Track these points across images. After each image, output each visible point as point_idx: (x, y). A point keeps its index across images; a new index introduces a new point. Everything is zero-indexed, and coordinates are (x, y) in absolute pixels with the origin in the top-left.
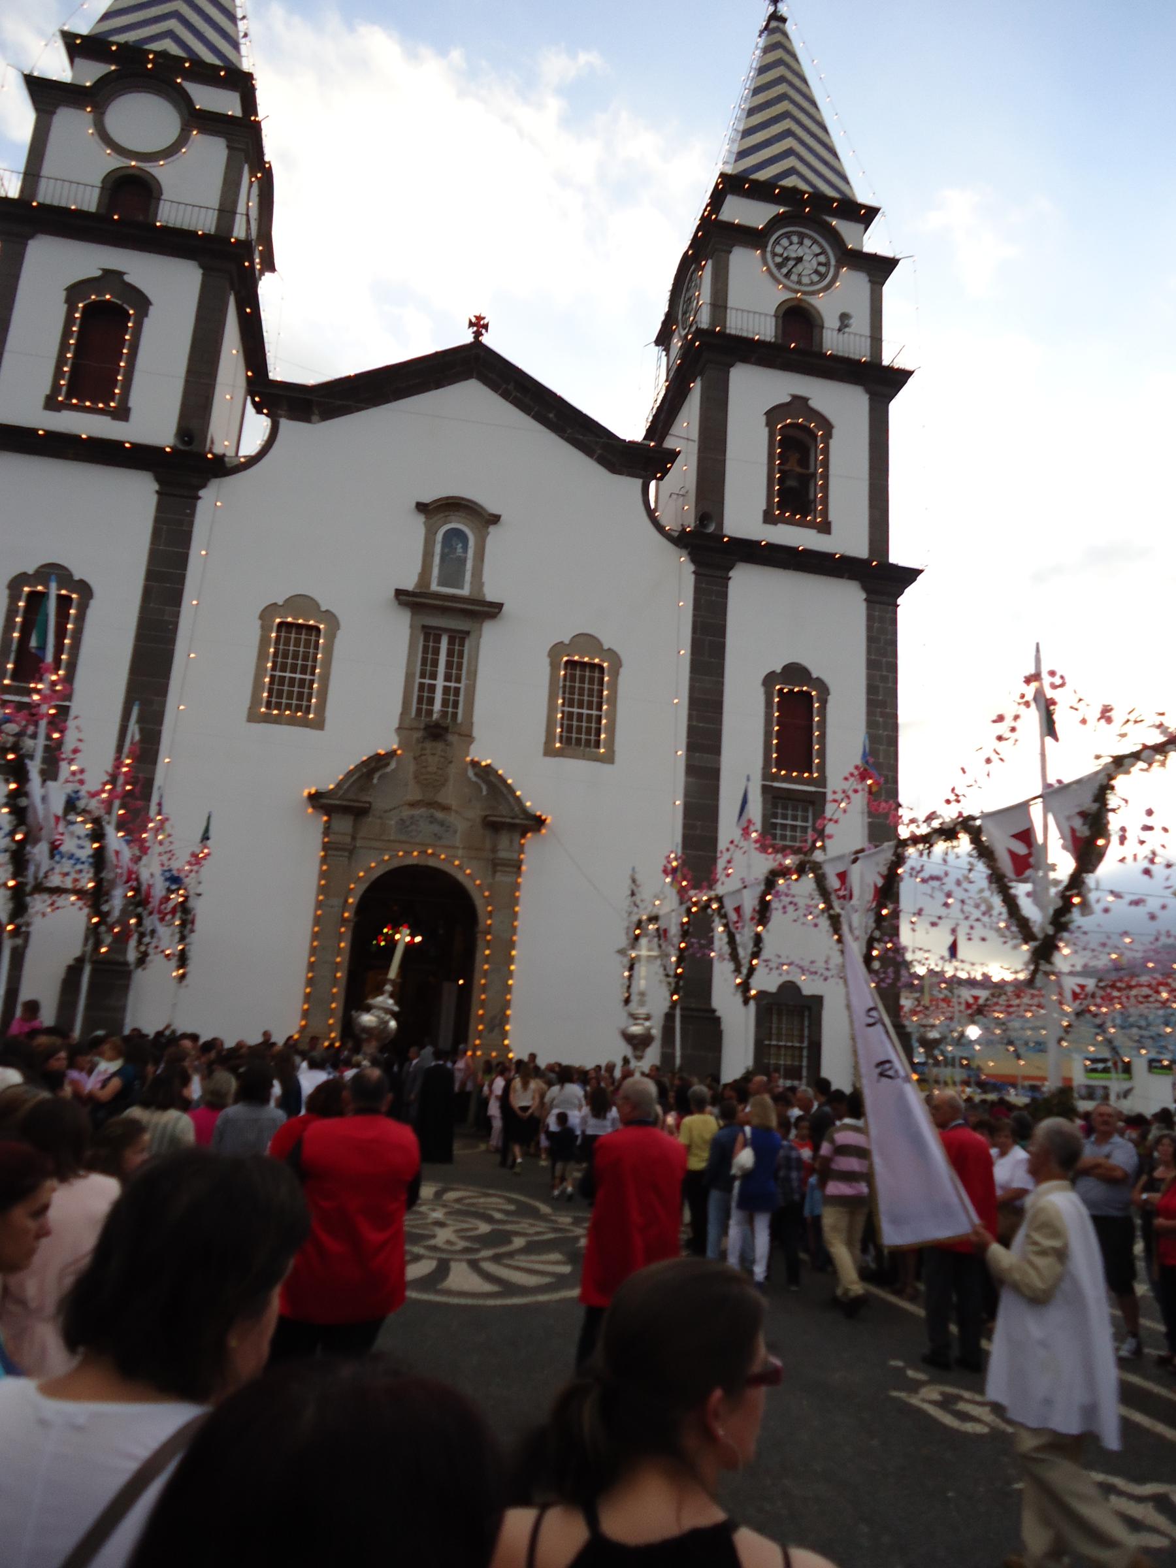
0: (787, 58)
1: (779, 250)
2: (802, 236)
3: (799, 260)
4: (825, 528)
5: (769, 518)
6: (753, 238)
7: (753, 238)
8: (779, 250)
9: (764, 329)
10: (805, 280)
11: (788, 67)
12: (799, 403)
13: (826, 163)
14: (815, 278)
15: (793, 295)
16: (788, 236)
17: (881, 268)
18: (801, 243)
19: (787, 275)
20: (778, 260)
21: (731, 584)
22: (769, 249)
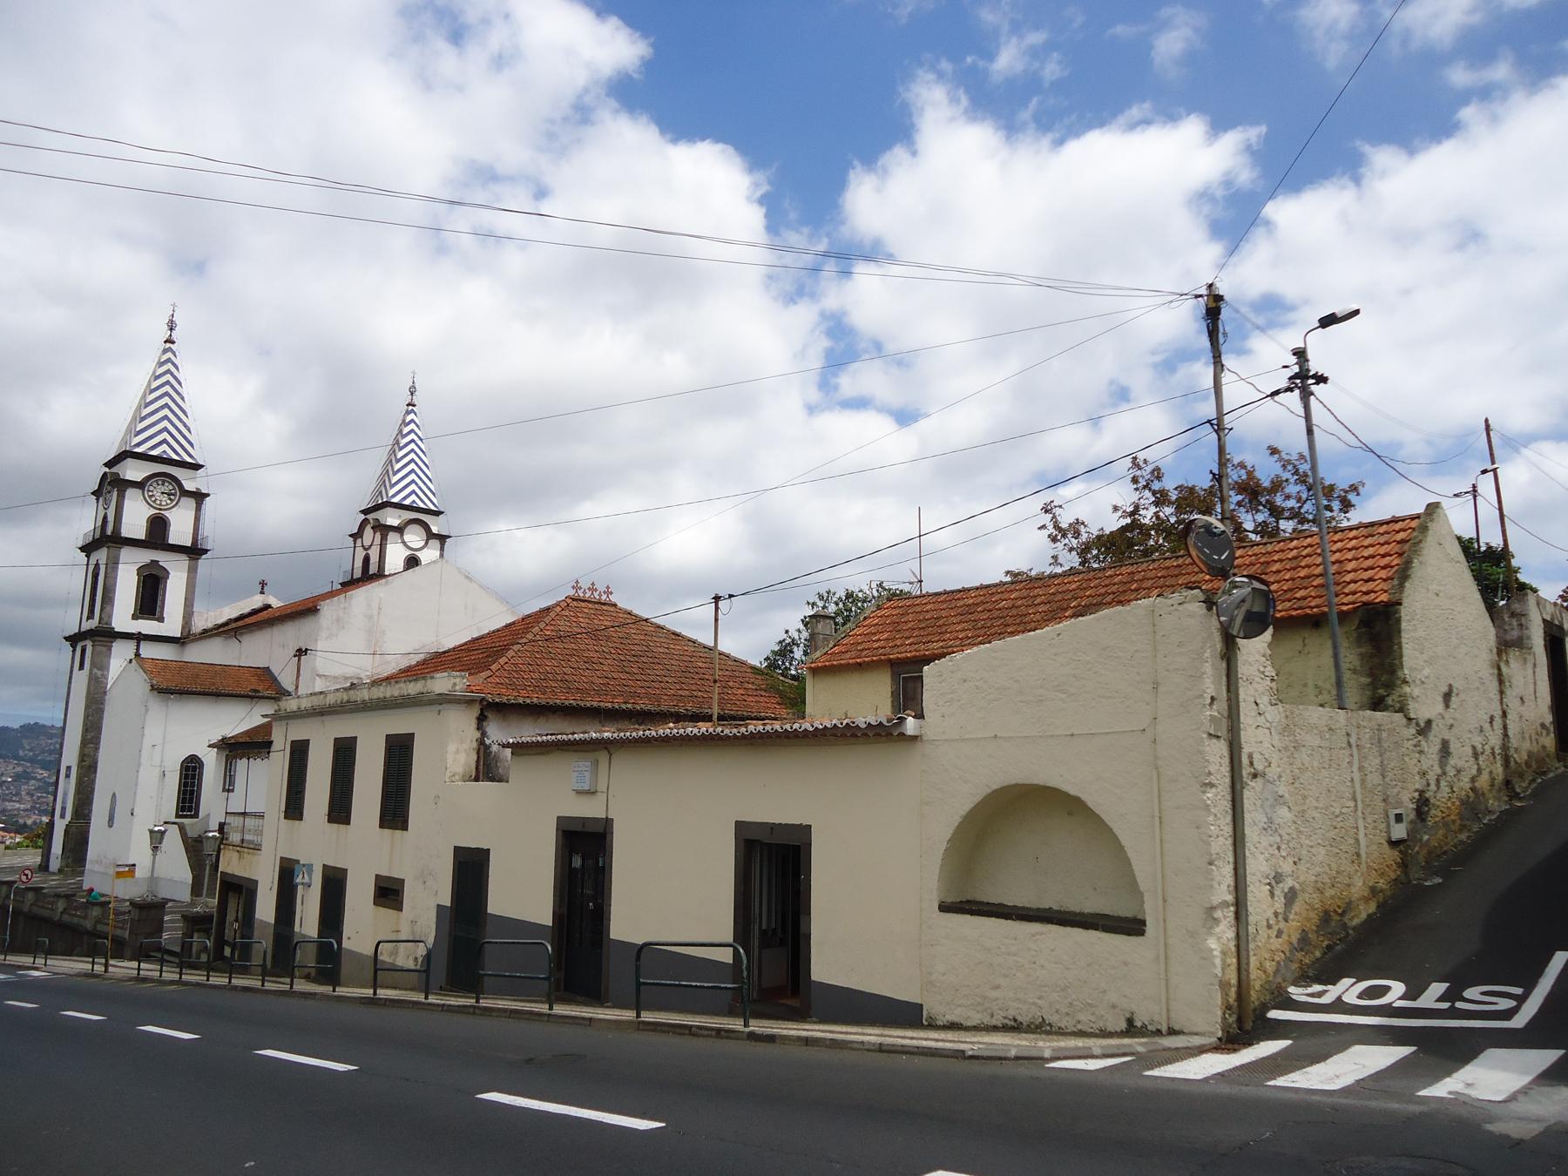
0: (173, 369)
1: (151, 488)
2: (164, 482)
3: (162, 493)
4: (161, 620)
5: (135, 617)
6: (140, 485)
7: (140, 485)
8: (151, 488)
9: (140, 533)
10: (164, 503)
11: (172, 374)
12: (154, 563)
13: (185, 437)
14: (169, 502)
15: (158, 512)
16: (157, 481)
17: (199, 497)
18: (163, 485)
19: (154, 502)
20: (150, 494)
21: (113, 649)
22: (146, 489)
